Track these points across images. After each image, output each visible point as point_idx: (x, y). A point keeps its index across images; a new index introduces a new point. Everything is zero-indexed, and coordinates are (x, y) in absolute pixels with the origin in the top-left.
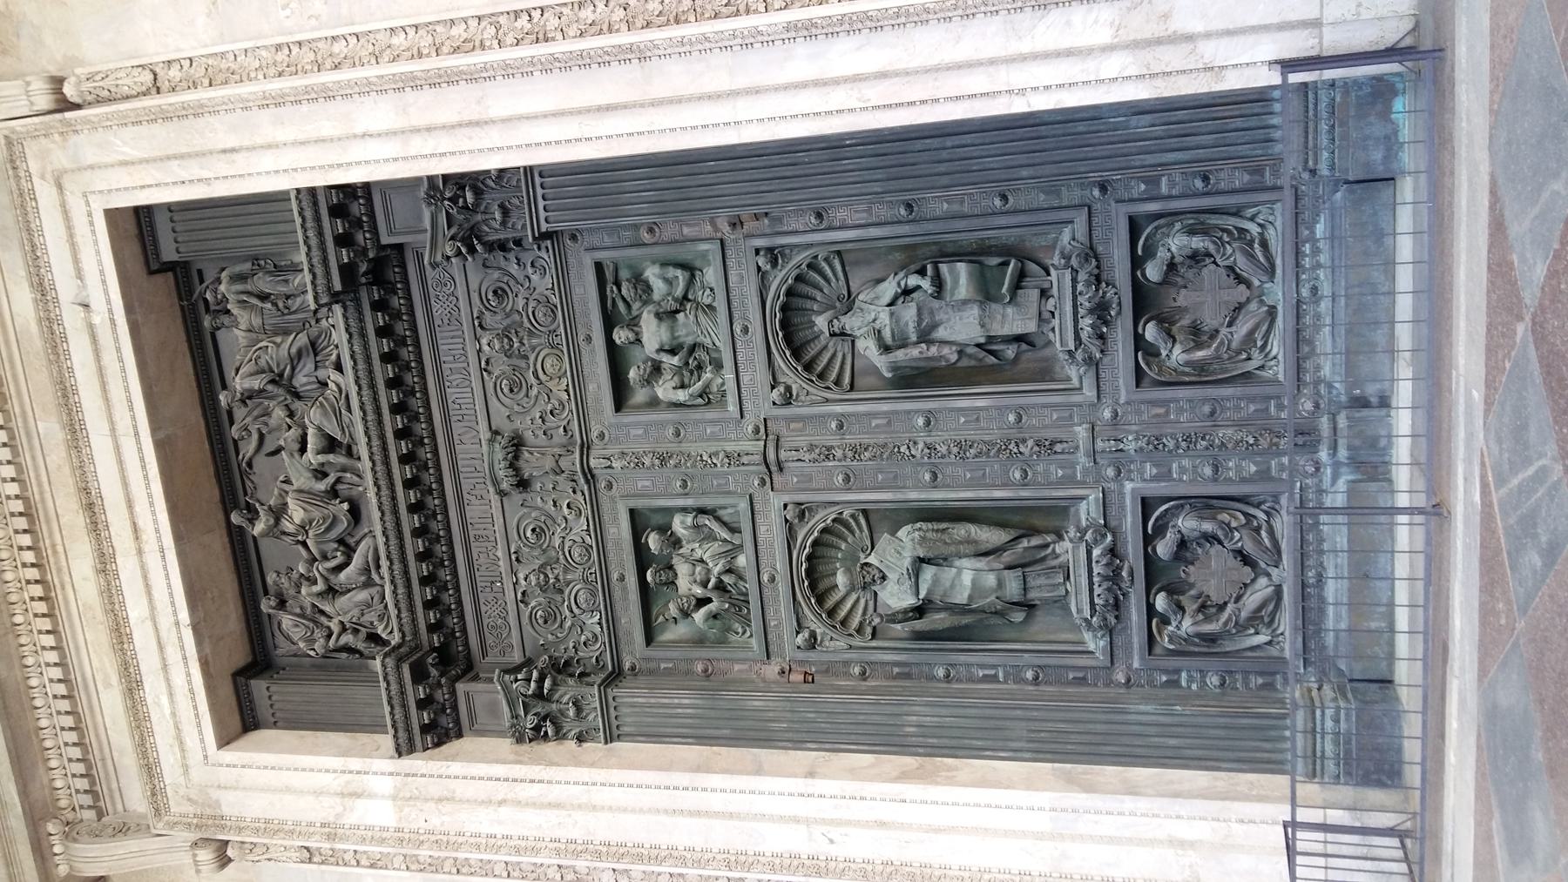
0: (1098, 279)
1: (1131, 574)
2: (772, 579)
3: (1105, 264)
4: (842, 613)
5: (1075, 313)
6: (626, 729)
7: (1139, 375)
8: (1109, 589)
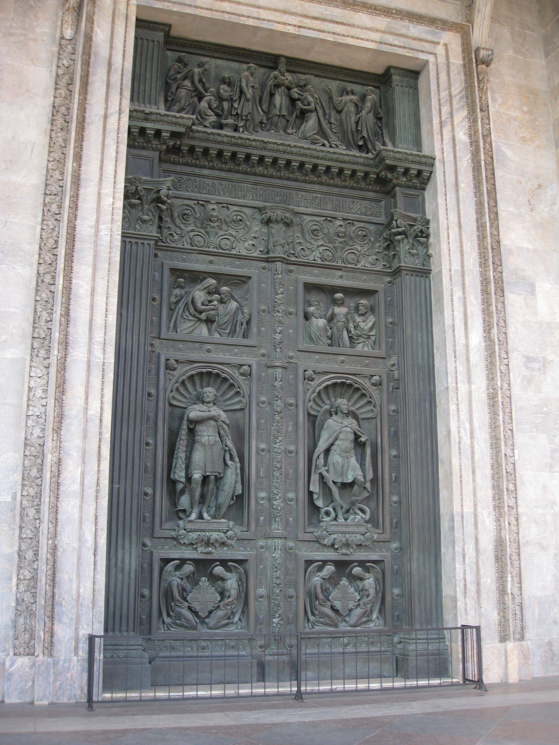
0: (361, 545)
1: (210, 553)
2: (209, 351)
4: (181, 390)
5: (345, 533)
6: (128, 247)
7: (309, 563)
8: (202, 540)
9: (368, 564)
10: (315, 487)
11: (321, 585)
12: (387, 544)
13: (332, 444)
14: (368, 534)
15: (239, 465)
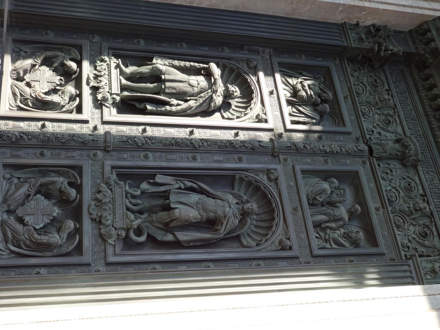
0: (100, 222)
3: (96, 232)
9: (78, 236)
10: (159, 179)
11: (54, 183)
12: (103, 261)
13: (208, 195)
14: (114, 229)
15: (174, 109)
